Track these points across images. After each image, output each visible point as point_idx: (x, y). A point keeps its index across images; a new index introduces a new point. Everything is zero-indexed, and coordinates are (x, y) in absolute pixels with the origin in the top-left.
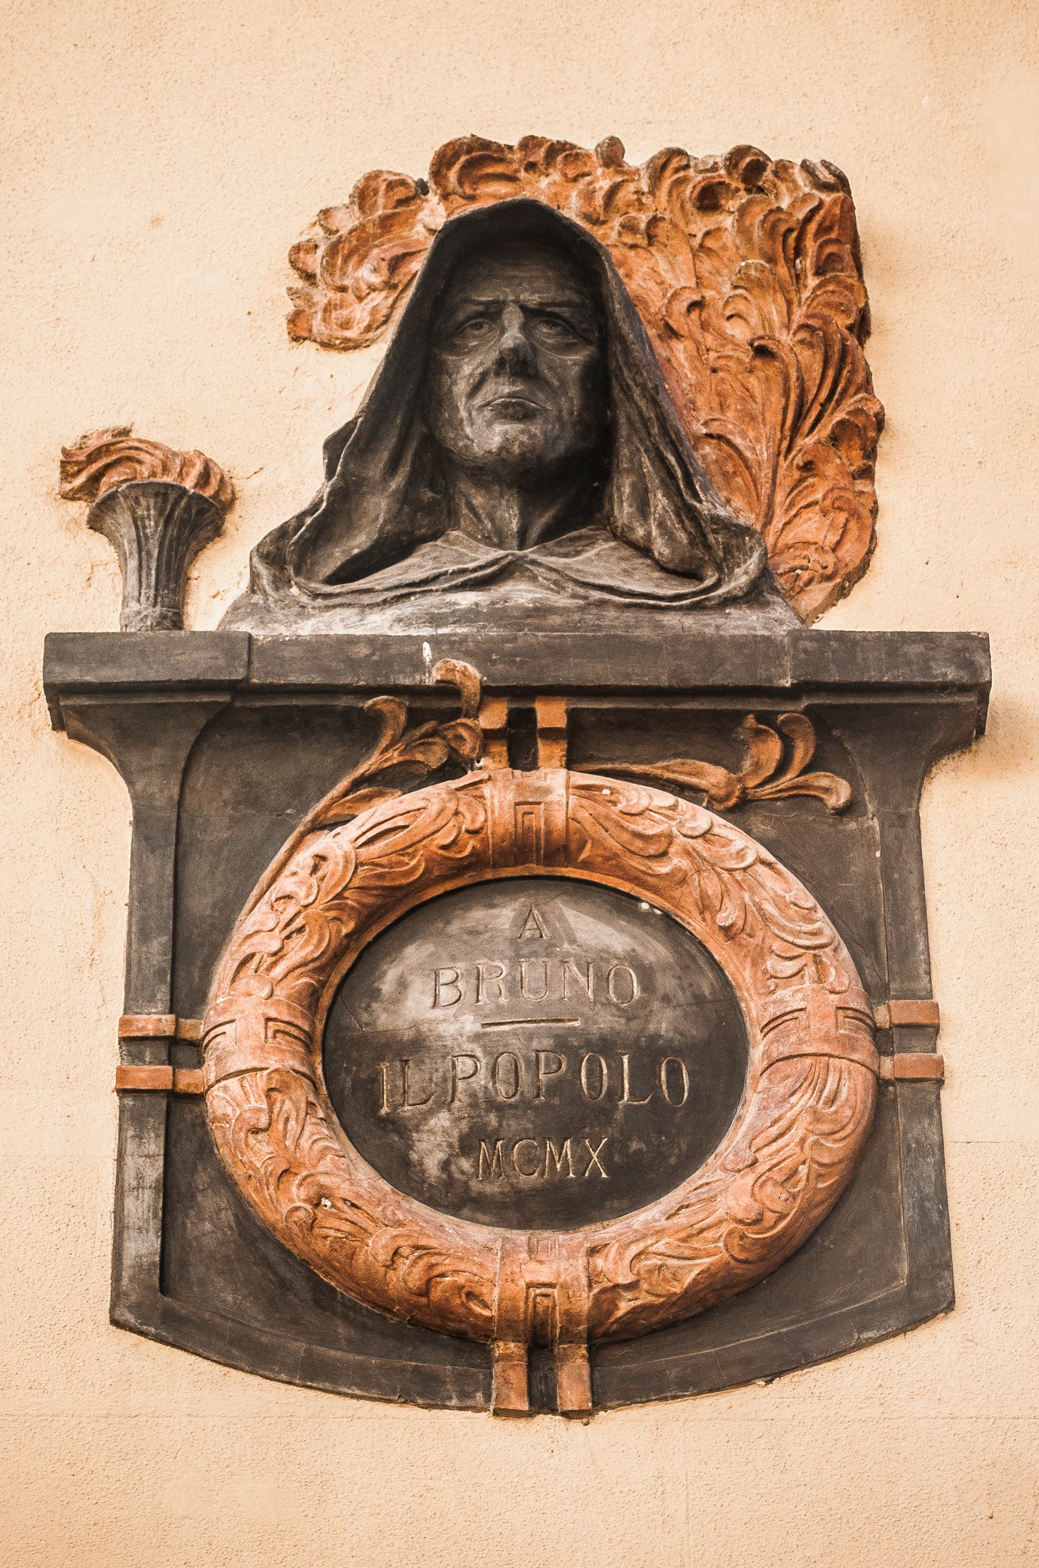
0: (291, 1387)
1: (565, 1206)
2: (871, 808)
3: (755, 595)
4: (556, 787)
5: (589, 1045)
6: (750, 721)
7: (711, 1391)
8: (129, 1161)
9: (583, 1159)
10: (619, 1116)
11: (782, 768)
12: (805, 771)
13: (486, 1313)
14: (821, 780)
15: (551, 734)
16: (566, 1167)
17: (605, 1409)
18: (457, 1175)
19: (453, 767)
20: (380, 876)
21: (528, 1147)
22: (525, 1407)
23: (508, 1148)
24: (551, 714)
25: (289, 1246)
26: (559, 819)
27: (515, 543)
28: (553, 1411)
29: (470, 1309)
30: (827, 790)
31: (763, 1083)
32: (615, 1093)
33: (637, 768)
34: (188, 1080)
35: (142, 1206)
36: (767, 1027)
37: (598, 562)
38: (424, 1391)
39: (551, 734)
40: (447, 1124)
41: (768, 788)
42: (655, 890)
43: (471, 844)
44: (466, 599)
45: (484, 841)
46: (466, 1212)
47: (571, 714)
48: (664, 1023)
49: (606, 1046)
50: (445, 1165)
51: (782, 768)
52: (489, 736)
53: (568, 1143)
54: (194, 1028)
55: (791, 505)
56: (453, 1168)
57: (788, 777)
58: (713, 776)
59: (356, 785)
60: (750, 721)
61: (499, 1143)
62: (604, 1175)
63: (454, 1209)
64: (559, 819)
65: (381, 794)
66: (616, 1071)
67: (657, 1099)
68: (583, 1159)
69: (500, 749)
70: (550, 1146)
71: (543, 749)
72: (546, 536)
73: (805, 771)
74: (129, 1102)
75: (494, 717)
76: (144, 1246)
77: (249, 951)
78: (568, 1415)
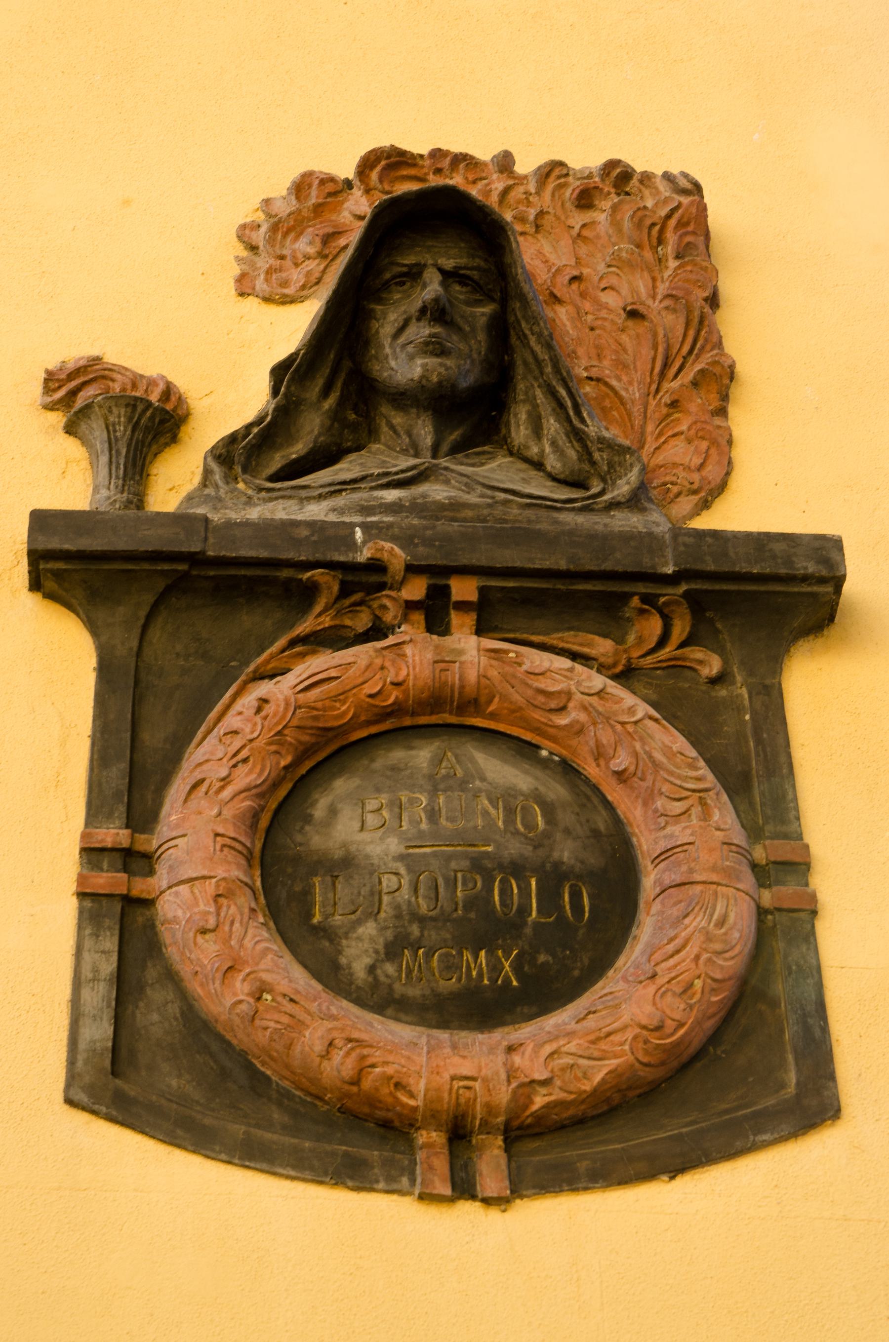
0: (229, 1167)
1: (481, 1009)
2: (739, 678)
3: (635, 501)
4: (468, 650)
5: (501, 867)
6: (635, 601)
7: (620, 1184)
8: (86, 956)
9: (495, 968)
10: (528, 931)
11: (662, 642)
12: (682, 645)
13: (412, 1103)
14: (696, 653)
15: (463, 606)
16: (480, 975)
17: (521, 1197)
18: (382, 979)
19: (376, 632)
20: (316, 718)
21: (447, 955)
22: (448, 1191)
23: (429, 955)
24: (464, 589)
25: (228, 1036)
26: (472, 676)
27: (429, 454)
28: (473, 1197)
29: (396, 1098)
30: (701, 662)
31: (656, 907)
32: (524, 910)
33: (535, 638)
34: (140, 887)
35: (98, 997)
36: (657, 859)
37: (499, 470)
38: (351, 1174)
39: (463, 606)
40: (374, 932)
41: (650, 659)
42: (553, 739)
43: (394, 696)
44: (391, 495)
45: (406, 692)
46: (389, 1011)
47: (482, 590)
48: (566, 852)
49: (516, 869)
50: (371, 969)
51: (662, 642)
52: (410, 606)
53: (483, 953)
54: (150, 843)
55: (660, 434)
56: (379, 972)
57: (667, 650)
58: (602, 647)
59: (292, 643)
60: (635, 601)
61: (421, 951)
62: (515, 983)
63: (379, 1009)
64: (472, 676)
65: (314, 652)
66: (525, 891)
67: (561, 917)
68: (495, 968)
69: (419, 617)
70: (467, 955)
71: (455, 618)
72: (456, 449)
73: (682, 645)
74: (88, 904)
75: (416, 589)
76: (99, 1032)
77: (199, 777)
78: (487, 1201)
